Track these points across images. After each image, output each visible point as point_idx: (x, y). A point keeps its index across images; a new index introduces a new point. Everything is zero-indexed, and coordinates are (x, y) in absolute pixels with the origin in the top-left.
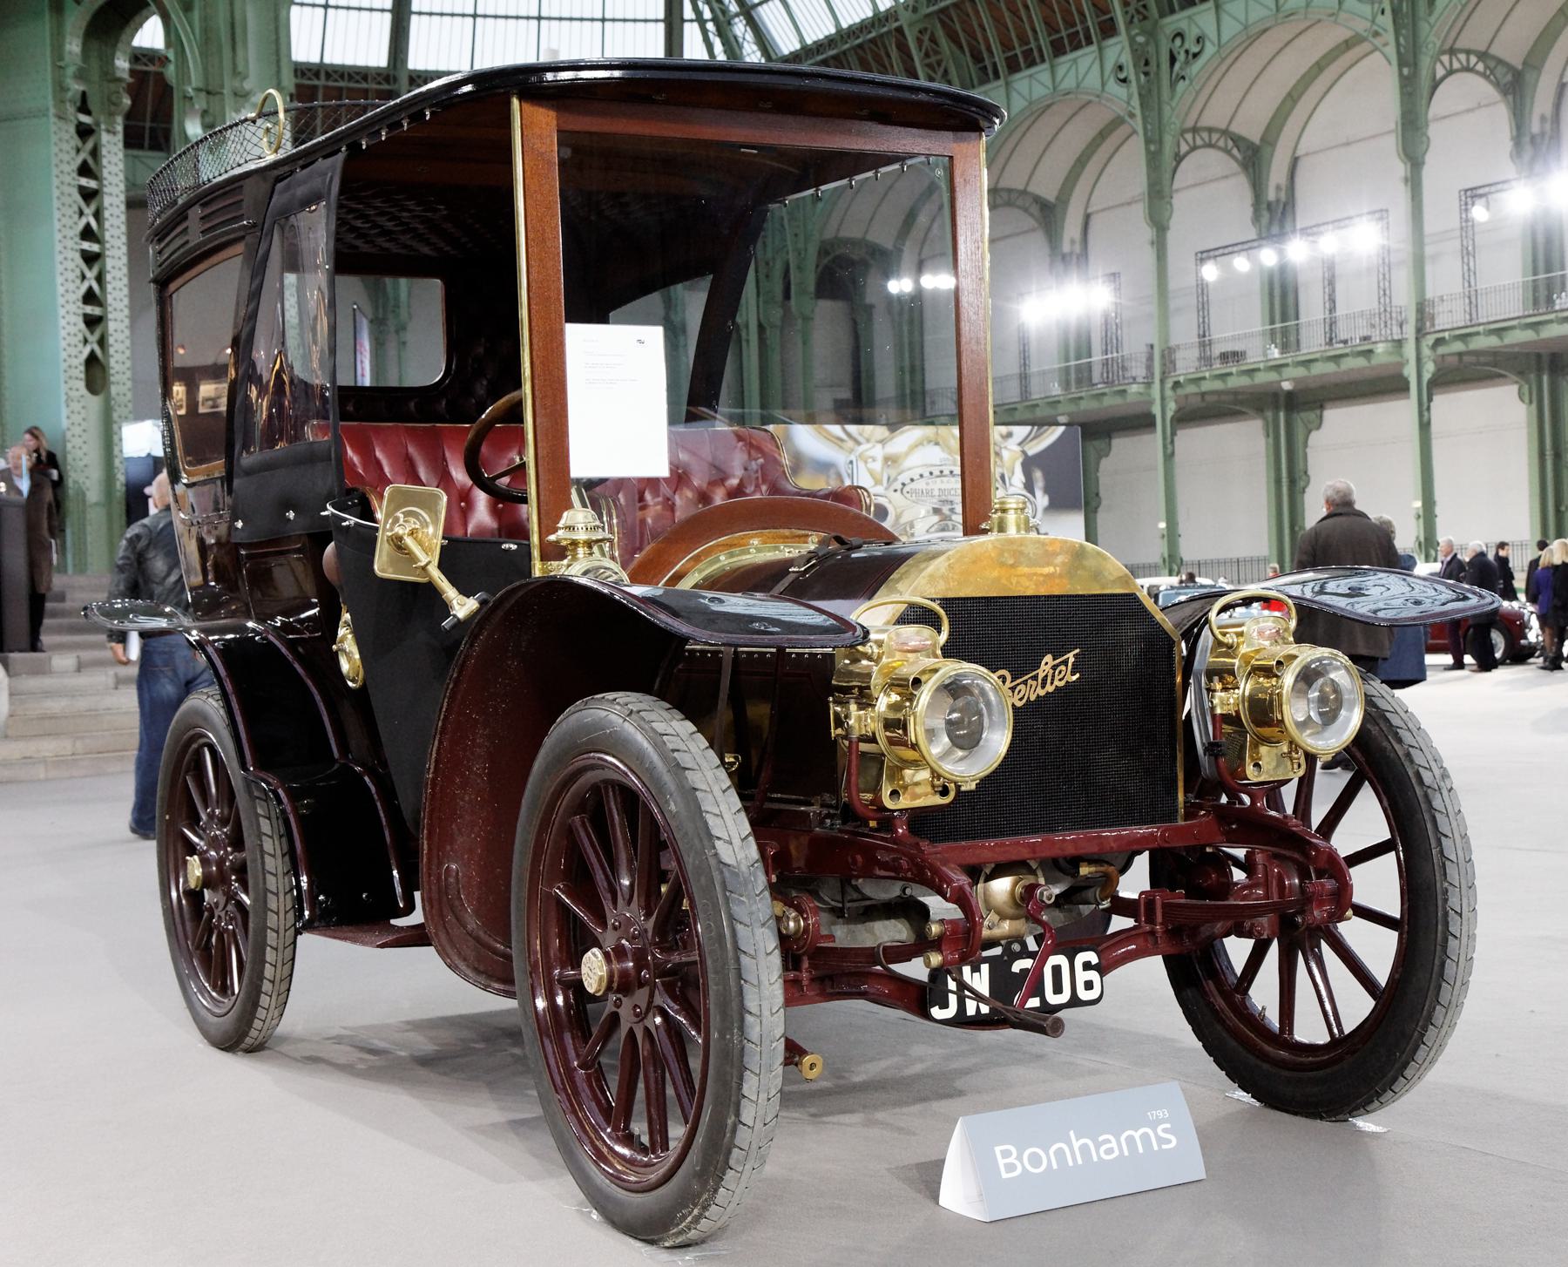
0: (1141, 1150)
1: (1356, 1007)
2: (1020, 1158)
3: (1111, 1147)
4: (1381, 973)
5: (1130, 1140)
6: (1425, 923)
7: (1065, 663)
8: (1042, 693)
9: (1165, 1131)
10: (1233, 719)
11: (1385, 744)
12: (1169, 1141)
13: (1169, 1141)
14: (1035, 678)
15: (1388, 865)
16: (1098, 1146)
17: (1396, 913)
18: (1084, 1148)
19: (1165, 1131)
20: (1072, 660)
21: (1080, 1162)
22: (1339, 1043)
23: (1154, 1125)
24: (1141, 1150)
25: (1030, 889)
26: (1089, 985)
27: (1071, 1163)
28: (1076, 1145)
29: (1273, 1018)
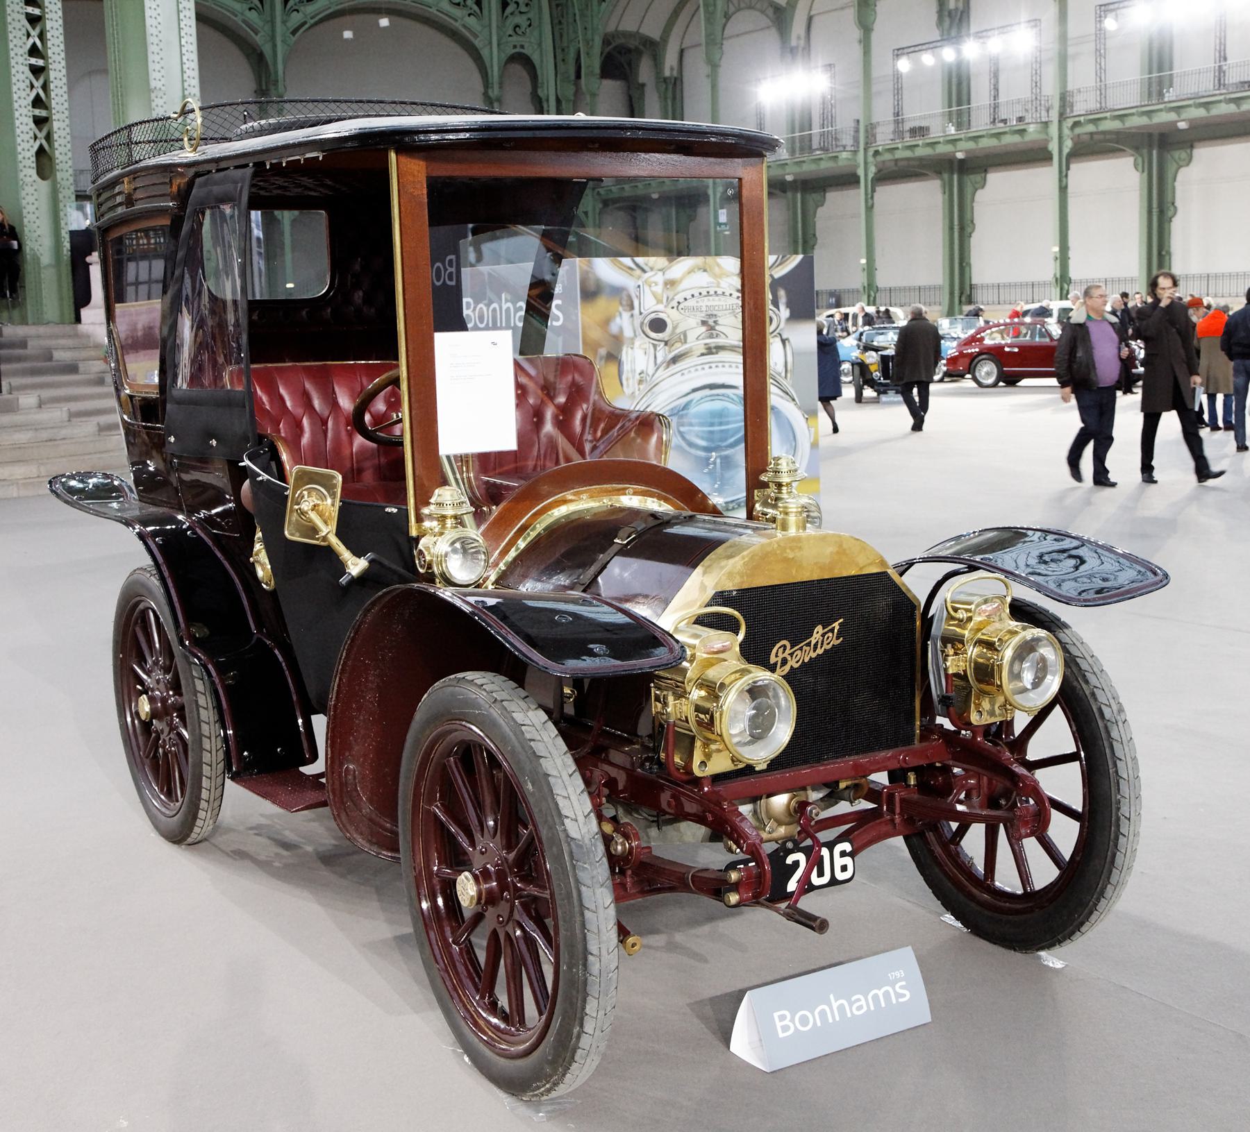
0: (883, 1005)
1: (1044, 873)
2: (792, 1020)
3: (861, 1005)
4: (1066, 849)
5: (876, 997)
6: (1101, 816)
7: (832, 630)
8: (814, 655)
9: (901, 987)
10: (963, 677)
11: (1075, 683)
12: (904, 996)
13: (904, 996)
14: (809, 644)
15: (1073, 770)
16: (851, 1005)
17: (1078, 806)
18: (841, 1008)
19: (901, 987)
20: (837, 628)
21: (837, 1018)
22: (1030, 896)
23: (893, 984)
24: (883, 1005)
25: (803, 805)
26: (844, 868)
27: (831, 1020)
28: (835, 1005)
29: (980, 866)
